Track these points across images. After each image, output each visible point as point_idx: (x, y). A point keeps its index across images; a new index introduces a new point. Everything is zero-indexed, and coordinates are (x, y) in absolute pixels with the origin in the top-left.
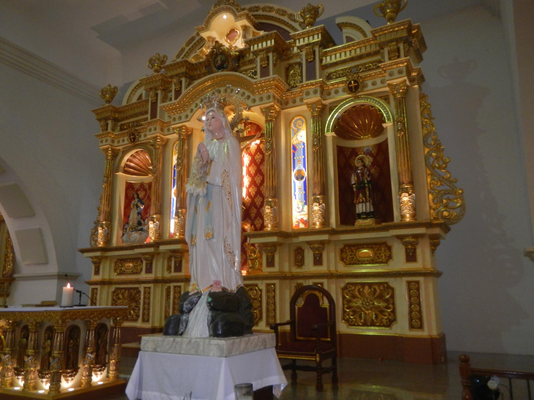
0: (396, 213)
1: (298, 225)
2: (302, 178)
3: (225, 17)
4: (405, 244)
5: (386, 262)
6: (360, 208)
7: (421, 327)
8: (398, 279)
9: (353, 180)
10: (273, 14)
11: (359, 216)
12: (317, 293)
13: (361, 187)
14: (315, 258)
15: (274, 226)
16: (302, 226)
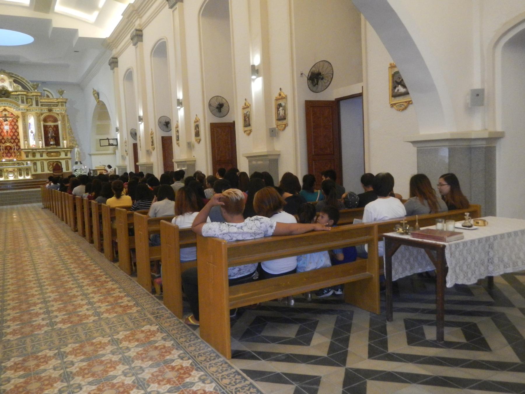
0: (61, 144)
1: (32, 145)
2: (33, 133)
3: (2, 76)
4: (65, 152)
5: (59, 156)
6: (52, 143)
7: (68, 170)
8: (63, 160)
9: (49, 135)
10: (19, 78)
11: (51, 145)
12: (58, 163)
13: (52, 137)
14: (40, 155)
15: (28, 147)
16: (33, 146)
